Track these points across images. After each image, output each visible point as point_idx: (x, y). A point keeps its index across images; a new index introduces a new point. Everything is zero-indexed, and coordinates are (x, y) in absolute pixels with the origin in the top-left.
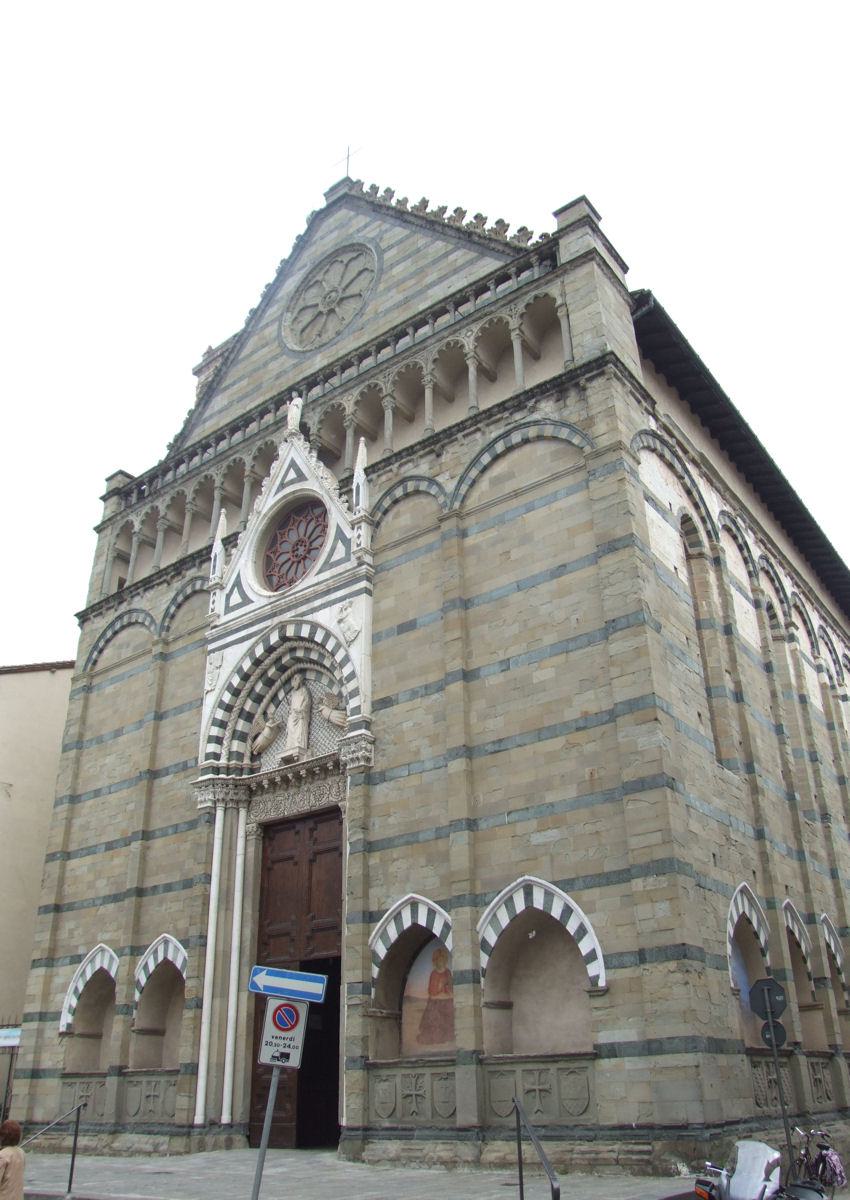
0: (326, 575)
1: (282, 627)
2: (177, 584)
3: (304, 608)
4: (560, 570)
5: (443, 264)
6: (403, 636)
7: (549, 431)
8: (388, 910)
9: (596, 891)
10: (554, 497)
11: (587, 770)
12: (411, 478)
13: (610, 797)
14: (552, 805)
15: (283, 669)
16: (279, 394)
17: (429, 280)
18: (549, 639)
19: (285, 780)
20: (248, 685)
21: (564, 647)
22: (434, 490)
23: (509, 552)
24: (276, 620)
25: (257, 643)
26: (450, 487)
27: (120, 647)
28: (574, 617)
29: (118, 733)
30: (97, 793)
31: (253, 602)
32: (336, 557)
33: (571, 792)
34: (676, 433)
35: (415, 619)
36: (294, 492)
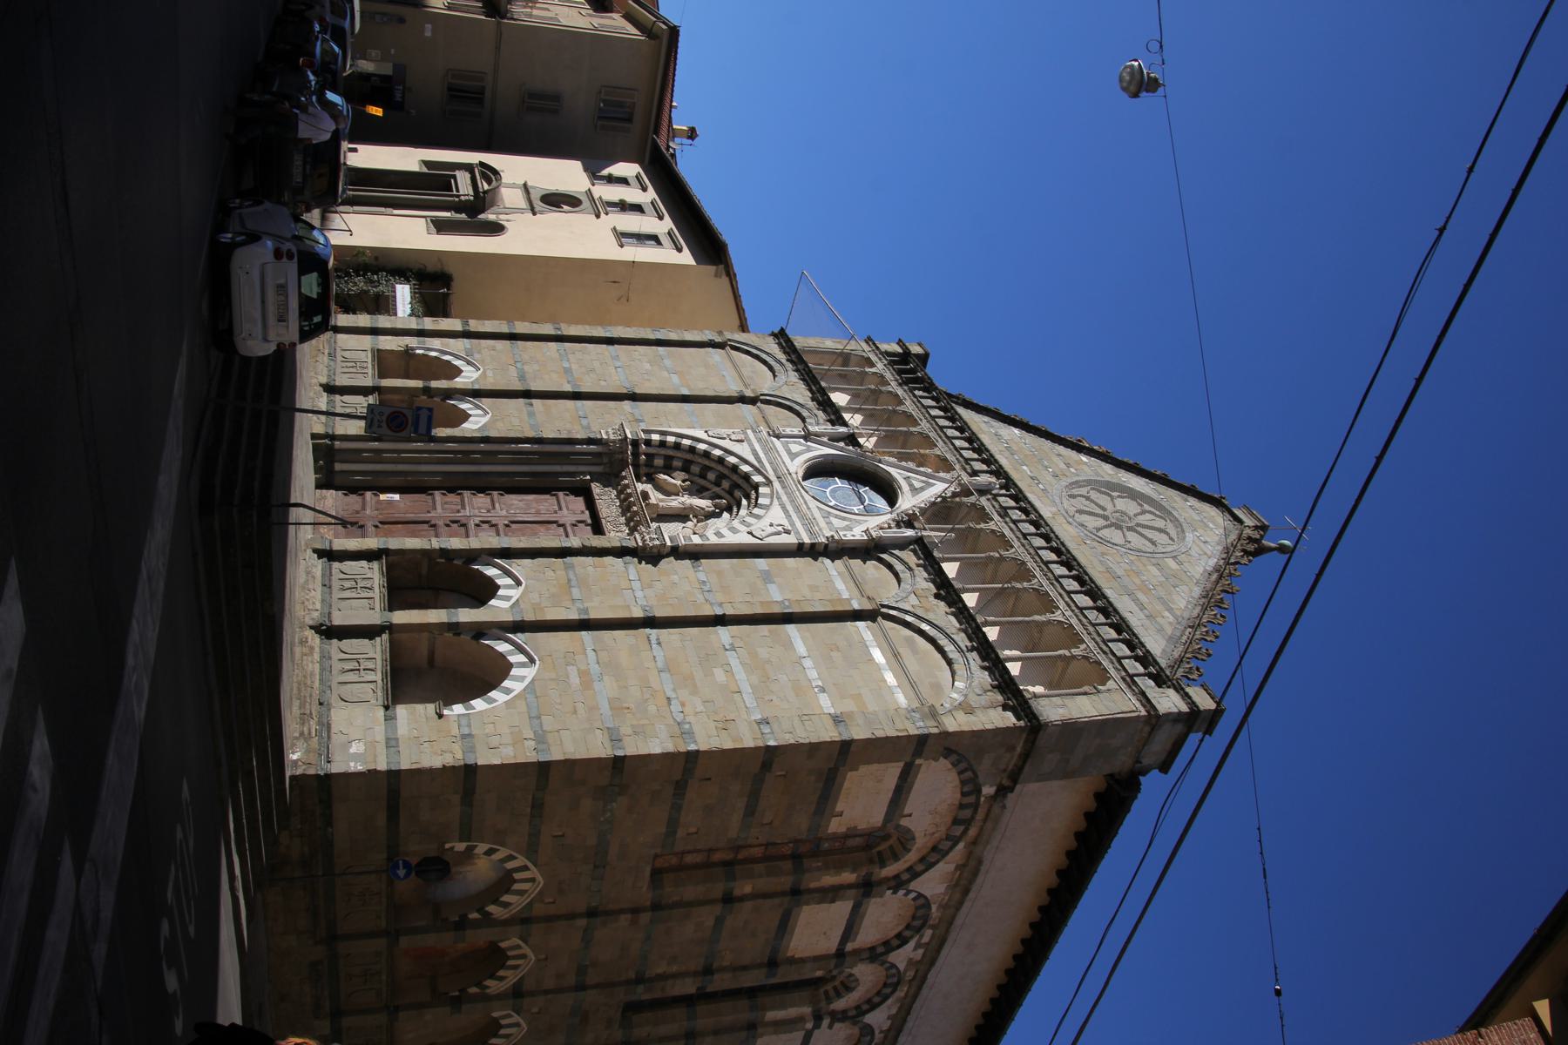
0: (817, 514)
1: (769, 483)
3: (784, 498)
11: (632, 706)
12: (913, 576)
15: (731, 493)
19: (630, 495)
20: (713, 465)
23: (839, 651)
25: (752, 465)
28: (774, 698)
31: (792, 461)
32: (835, 521)
34: (989, 825)
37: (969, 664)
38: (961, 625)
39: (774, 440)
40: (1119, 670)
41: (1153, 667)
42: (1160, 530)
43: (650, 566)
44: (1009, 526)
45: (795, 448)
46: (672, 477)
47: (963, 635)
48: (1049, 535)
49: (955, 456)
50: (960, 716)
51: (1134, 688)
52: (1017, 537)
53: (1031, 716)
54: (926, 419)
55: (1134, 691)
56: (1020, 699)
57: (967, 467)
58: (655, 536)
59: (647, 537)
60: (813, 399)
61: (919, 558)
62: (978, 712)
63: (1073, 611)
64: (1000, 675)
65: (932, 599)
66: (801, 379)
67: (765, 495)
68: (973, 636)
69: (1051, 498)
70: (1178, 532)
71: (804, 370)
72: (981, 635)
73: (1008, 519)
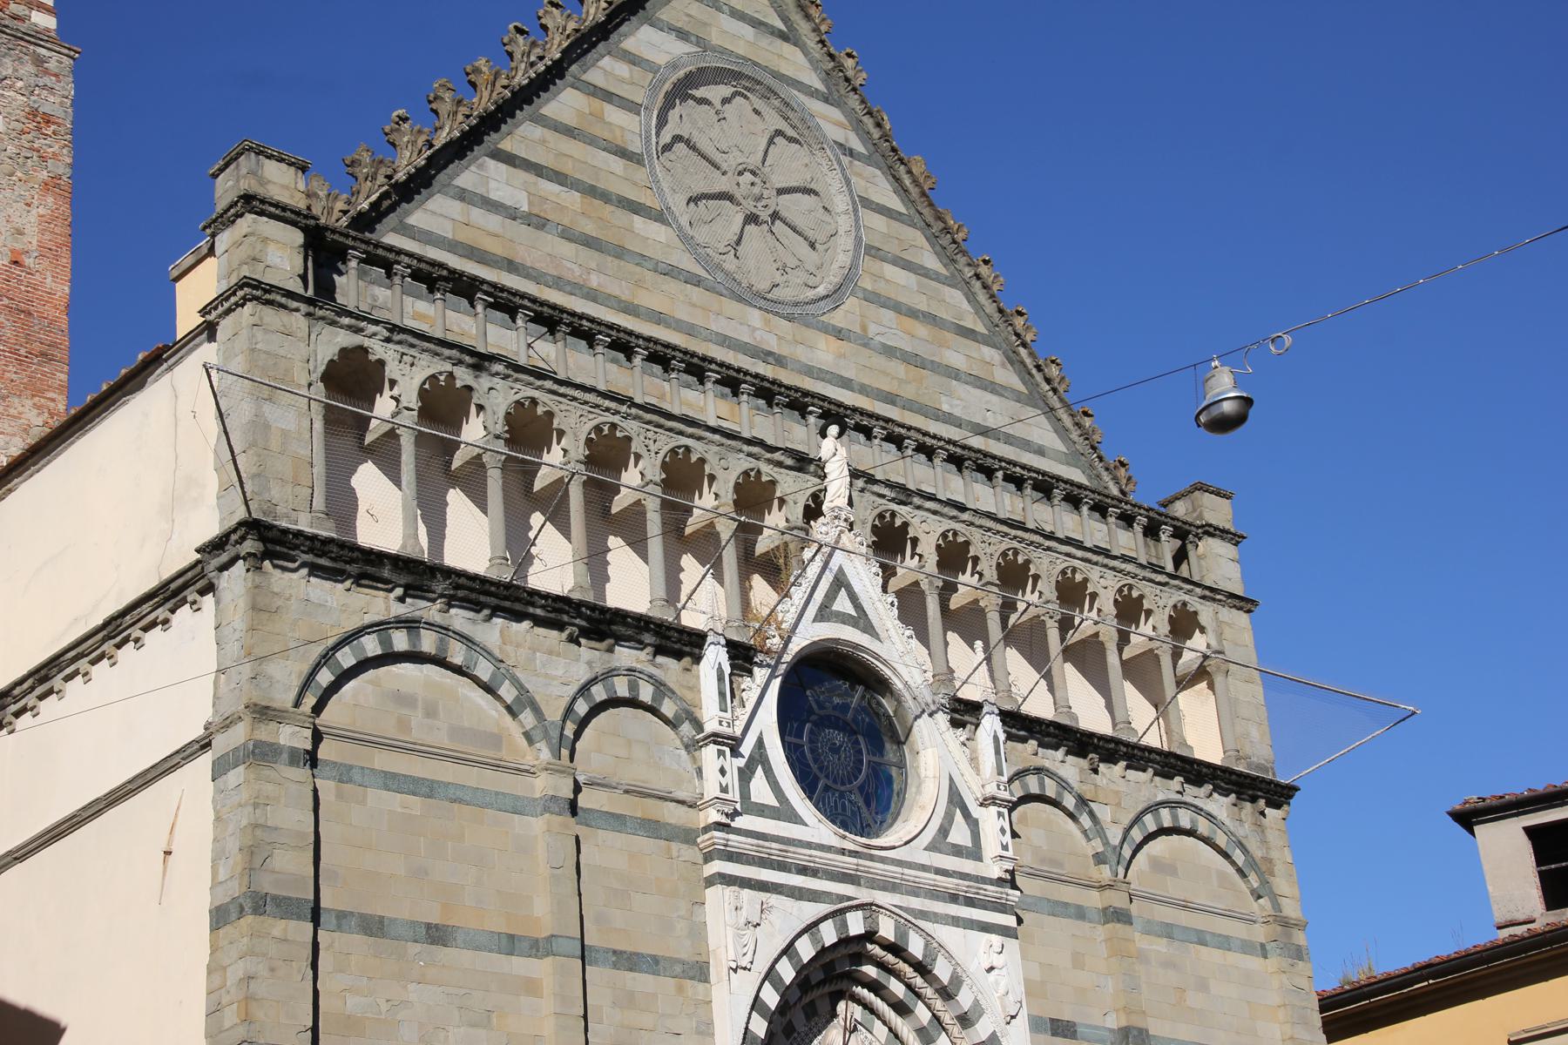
7: (1221, 840)
10: (1224, 943)
16: (773, 382)
22: (1085, 820)
24: (864, 895)
27: (403, 699)
29: (437, 935)
36: (857, 646)
37: (1201, 810)
38: (1144, 771)
39: (740, 822)
41: (1166, 524)
44: (928, 510)
49: (741, 451)
50: (1283, 884)
51: (1218, 597)
54: (617, 412)
55: (1220, 601)
57: (778, 456)
61: (1023, 740)
62: (1274, 854)
63: (1096, 564)
64: (1226, 784)
66: (488, 619)
67: (901, 933)
69: (724, 292)
71: (457, 587)
73: (917, 500)
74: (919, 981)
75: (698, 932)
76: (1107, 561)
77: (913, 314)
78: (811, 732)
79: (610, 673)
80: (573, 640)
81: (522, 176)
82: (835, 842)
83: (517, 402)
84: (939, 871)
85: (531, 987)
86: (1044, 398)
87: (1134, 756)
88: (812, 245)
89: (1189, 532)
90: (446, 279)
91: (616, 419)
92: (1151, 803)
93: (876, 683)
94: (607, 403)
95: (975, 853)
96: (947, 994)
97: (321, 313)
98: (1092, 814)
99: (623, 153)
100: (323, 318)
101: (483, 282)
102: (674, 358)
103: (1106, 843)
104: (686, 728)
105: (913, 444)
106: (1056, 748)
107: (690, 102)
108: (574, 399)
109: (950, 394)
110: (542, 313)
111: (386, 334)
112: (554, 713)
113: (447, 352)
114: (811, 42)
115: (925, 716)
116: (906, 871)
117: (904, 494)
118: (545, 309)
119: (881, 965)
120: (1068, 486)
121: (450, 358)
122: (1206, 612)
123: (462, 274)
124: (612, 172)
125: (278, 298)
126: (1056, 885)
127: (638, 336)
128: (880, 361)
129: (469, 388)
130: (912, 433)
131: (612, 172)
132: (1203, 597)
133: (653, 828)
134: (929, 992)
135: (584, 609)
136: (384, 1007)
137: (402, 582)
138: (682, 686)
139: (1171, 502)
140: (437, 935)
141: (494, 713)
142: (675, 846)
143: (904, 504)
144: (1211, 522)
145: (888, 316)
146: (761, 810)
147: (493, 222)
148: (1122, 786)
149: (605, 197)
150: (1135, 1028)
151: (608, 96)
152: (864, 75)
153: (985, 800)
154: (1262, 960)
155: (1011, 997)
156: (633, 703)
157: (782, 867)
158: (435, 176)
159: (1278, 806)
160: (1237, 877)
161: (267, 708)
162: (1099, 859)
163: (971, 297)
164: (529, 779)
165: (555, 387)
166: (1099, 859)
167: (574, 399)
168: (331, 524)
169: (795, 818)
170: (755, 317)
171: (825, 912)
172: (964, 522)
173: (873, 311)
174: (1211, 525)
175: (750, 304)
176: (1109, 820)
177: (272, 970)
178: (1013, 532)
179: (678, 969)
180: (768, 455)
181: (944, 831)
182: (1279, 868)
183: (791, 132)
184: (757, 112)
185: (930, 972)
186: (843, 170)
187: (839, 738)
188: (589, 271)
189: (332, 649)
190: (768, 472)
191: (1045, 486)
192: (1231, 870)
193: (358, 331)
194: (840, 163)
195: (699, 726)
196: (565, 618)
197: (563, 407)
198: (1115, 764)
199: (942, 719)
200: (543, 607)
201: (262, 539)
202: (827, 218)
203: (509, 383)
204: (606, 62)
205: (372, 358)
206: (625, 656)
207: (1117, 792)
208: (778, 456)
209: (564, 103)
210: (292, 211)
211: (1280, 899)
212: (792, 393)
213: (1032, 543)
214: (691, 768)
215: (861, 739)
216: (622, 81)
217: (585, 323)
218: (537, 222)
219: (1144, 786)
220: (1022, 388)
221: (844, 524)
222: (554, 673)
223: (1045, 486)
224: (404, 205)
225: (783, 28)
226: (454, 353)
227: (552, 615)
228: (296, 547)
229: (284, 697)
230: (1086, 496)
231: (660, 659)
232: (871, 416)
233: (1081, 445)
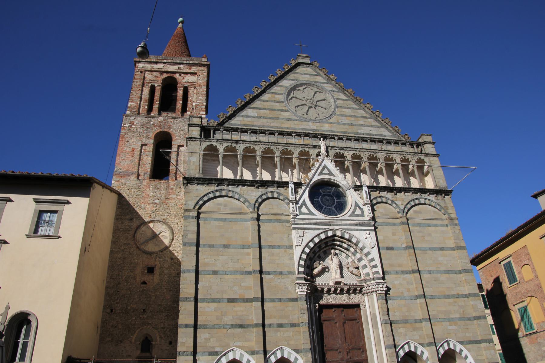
1: (333, 230)
2: (261, 191)
4: (442, 249)
5: (366, 120)
6: (389, 251)
7: (433, 204)
8: (400, 345)
9: (470, 345)
10: (436, 225)
11: (462, 310)
13: (469, 319)
14: (452, 318)
17: (361, 122)
18: (443, 269)
21: (448, 272)
22: (394, 205)
23: (424, 237)
25: (321, 233)
26: (402, 207)
27: (219, 204)
29: (226, 246)
30: (215, 273)
33: (457, 316)
35: (393, 247)
36: (329, 179)
37: (427, 199)
38: (410, 193)
39: (298, 217)
40: (421, 155)
42: (315, 93)
43: (390, 290)
45: (304, 210)
46: (316, 268)
47: (414, 194)
48: (348, 138)
49: (299, 147)
51: (429, 155)
52: (355, 151)
53: (449, 192)
54: (269, 145)
55: (429, 156)
56: (443, 191)
57: (308, 146)
58: (381, 286)
59: (382, 289)
60: (258, 188)
61: (376, 191)
62: (448, 205)
63: (394, 154)
65: (397, 196)
68: (415, 192)
70: (317, 88)
71: (229, 182)
72: (417, 190)
73: (345, 149)
74: (349, 243)
75: (290, 240)
76: (397, 153)
77: (350, 116)
78: (321, 197)
79: (267, 193)
80: (256, 188)
81: (255, 110)
82: (324, 218)
83: (246, 147)
84: (352, 220)
85: (248, 254)
86: (385, 126)
87: (406, 190)
88: (325, 109)
89: (421, 144)
90: (231, 129)
91: (269, 146)
92: (412, 199)
93: (337, 186)
94: (266, 144)
95: (363, 215)
96: (356, 245)
97: (202, 140)
98: (396, 204)
99: (278, 102)
100: (203, 141)
101: (239, 128)
102: (284, 133)
103: (400, 209)
104: (286, 201)
105: (345, 139)
106: (385, 192)
107: (296, 91)
108: (259, 144)
109: (361, 129)
110: (252, 131)
111: (216, 141)
112: (253, 202)
113: (229, 141)
114: (323, 75)
115: (348, 190)
116: (342, 221)
117: (342, 148)
118: (253, 130)
119: (340, 241)
120: (387, 140)
121: (230, 142)
122: (426, 159)
123: (234, 128)
124: (277, 106)
125: (194, 139)
126: (387, 219)
127: (275, 131)
128: (343, 126)
129: (235, 147)
130: (344, 137)
131: (277, 106)
132: (425, 156)
133: (279, 221)
134: (352, 245)
135: (259, 182)
136: (214, 261)
137: (217, 183)
138: (285, 193)
139: (419, 140)
140: (226, 246)
141: (240, 204)
142: (284, 224)
143: (342, 150)
144: (425, 141)
145: (344, 118)
146: (304, 214)
147: (249, 119)
148: (404, 197)
149: (275, 110)
150: (409, 246)
151: (276, 93)
152: (336, 78)
153: (364, 204)
154: (446, 228)
155: (372, 243)
156: (273, 198)
157: (311, 224)
158: (236, 114)
159: (448, 195)
160: (439, 211)
161: (187, 209)
162: (399, 212)
163: (365, 111)
164: (248, 215)
165: (254, 143)
166: (399, 212)
167: (259, 144)
168: (202, 175)
169: (313, 214)
170: (310, 124)
171: (321, 232)
172: (358, 151)
173: (340, 117)
174: (425, 142)
175: (309, 122)
176: (400, 204)
177: (187, 256)
178: (371, 151)
179: (285, 247)
180: (306, 146)
181: (354, 212)
182: (450, 208)
183: (319, 91)
184: (312, 89)
185: (351, 241)
186: (332, 95)
187: (328, 198)
188: (271, 123)
189: (202, 197)
190: (307, 150)
191: (389, 142)
192: (437, 210)
193: (211, 141)
194: (331, 93)
195: (288, 199)
196: (255, 184)
197: (257, 146)
198: (402, 193)
199: (352, 190)
200: (249, 183)
201: (187, 180)
202: (329, 104)
203: (244, 144)
204: (275, 88)
205: (214, 146)
206: (270, 189)
207: (403, 198)
208: (308, 146)
209: (266, 96)
210: (197, 125)
211: (450, 214)
212: (313, 134)
213: (377, 152)
214: (288, 208)
215: (334, 197)
216: (279, 90)
217: (262, 131)
218: (259, 117)
219: (409, 196)
220: (379, 125)
221: (325, 156)
222: (253, 195)
223: (389, 142)
224: (230, 120)
225: (316, 74)
226: (231, 141)
227: (252, 184)
228: (194, 180)
229: (192, 207)
230: (392, 141)
231: (279, 188)
232: (333, 135)
233: (395, 133)
